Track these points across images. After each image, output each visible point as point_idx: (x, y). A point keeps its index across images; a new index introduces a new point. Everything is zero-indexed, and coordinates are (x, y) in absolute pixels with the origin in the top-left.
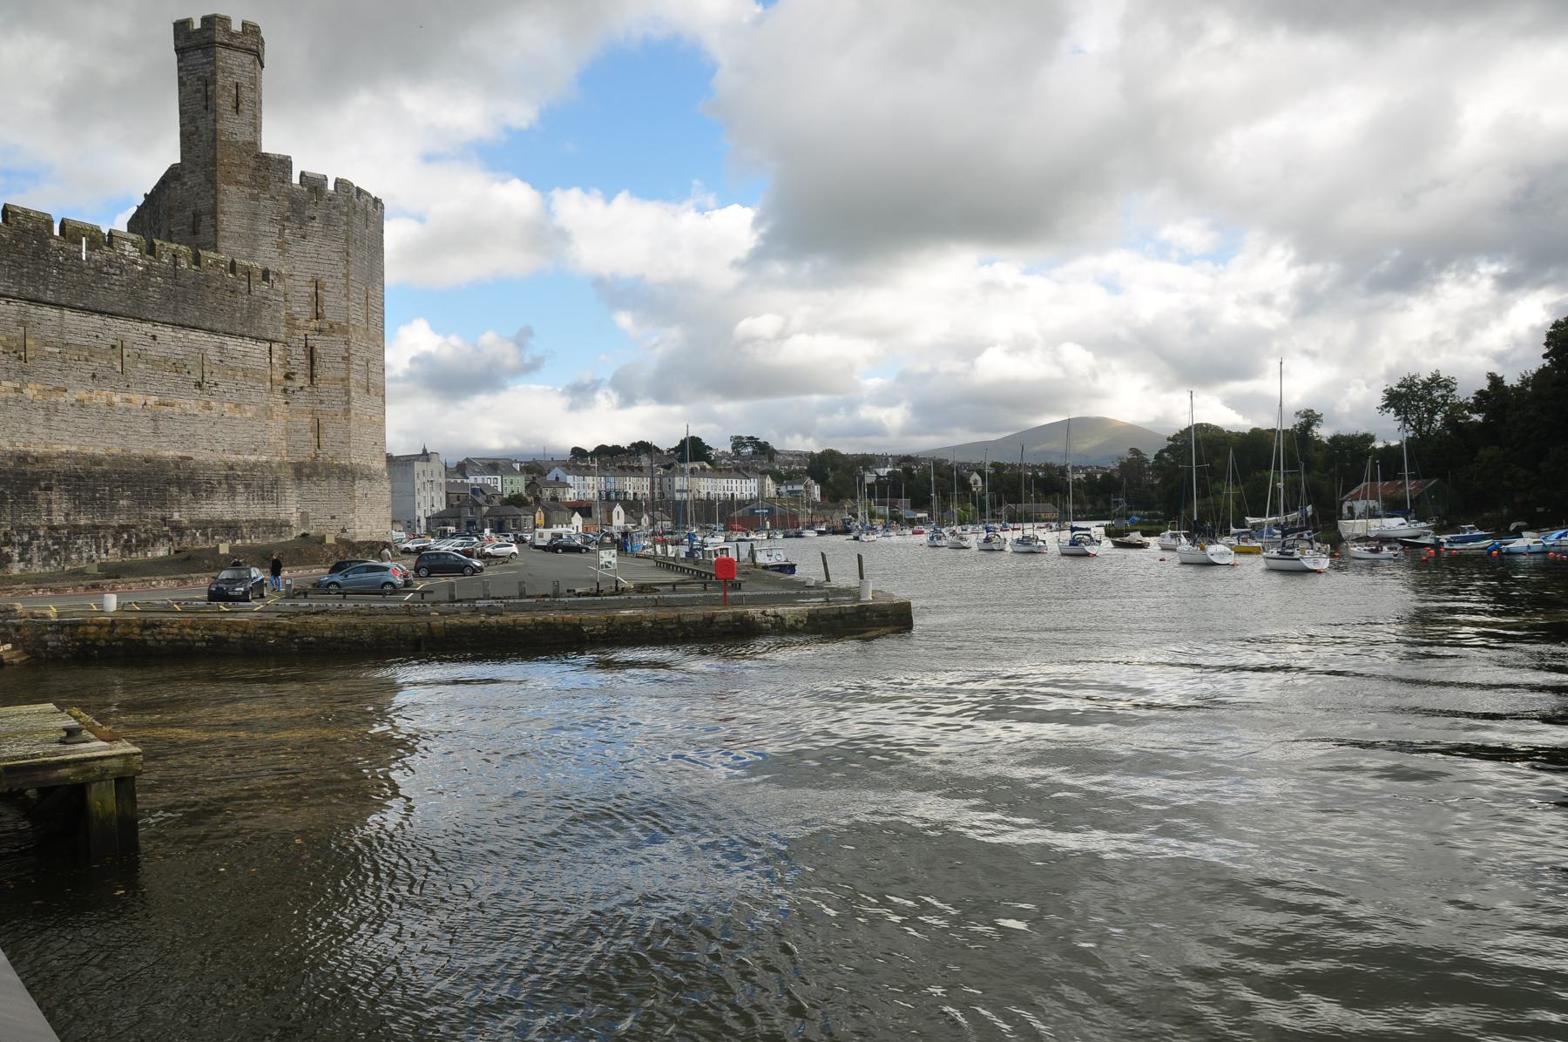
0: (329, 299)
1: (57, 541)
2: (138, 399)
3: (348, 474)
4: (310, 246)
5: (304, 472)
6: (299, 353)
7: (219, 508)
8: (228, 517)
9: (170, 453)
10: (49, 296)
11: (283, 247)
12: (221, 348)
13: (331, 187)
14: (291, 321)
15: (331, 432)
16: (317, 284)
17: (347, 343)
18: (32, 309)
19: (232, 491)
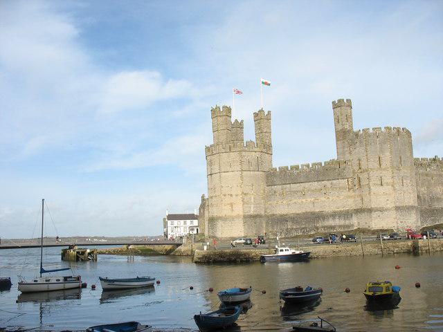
0: (362, 163)
2: (309, 200)
3: (370, 211)
5: (358, 211)
6: (356, 181)
7: (331, 222)
9: (317, 210)
11: (350, 153)
14: (354, 172)
15: (365, 199)
16: (359, 160)
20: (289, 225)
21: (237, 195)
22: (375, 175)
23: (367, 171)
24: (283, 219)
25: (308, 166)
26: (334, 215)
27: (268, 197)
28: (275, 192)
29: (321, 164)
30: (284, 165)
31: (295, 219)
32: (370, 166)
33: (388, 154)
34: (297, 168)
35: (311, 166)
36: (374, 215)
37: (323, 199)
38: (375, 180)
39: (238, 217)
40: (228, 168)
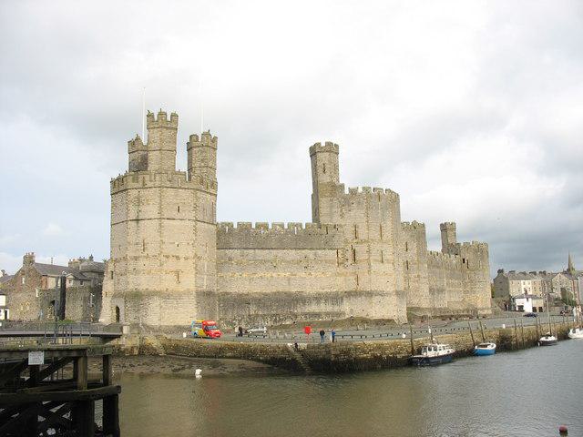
1: (250, 319)
3: (370, 294)
4: (352, 213)
5: (349, 294)
6: (349, 254)
7: (313, 308)
8: (317, 311)
9: (294, 291)
10: (251, 246)
11: (342, 216)
12: (315, 254)
13: (360, 190)
14: (346, 242)
15: (363, 280)
17: (369, 246)
18: (245, 251)
19: (318, 303)
20: (253, 310)
21: (186, 259)
22: (376, 247)
23: (365, 241)
24: (242, 301)
25: (282, 226)
26: (318, 298)
27: (221, 265)
28: (230, 259)
29: (301, 225)
30: (245, 220)
31: (262, 301)
32: (371, 236)
33: (389, 223)
34: (265, 226)
35: (286, 227)
36: (375, 299)
37: (303, 275)
38: (375, 256)
39: (188, 292)
40: (174, 214)
